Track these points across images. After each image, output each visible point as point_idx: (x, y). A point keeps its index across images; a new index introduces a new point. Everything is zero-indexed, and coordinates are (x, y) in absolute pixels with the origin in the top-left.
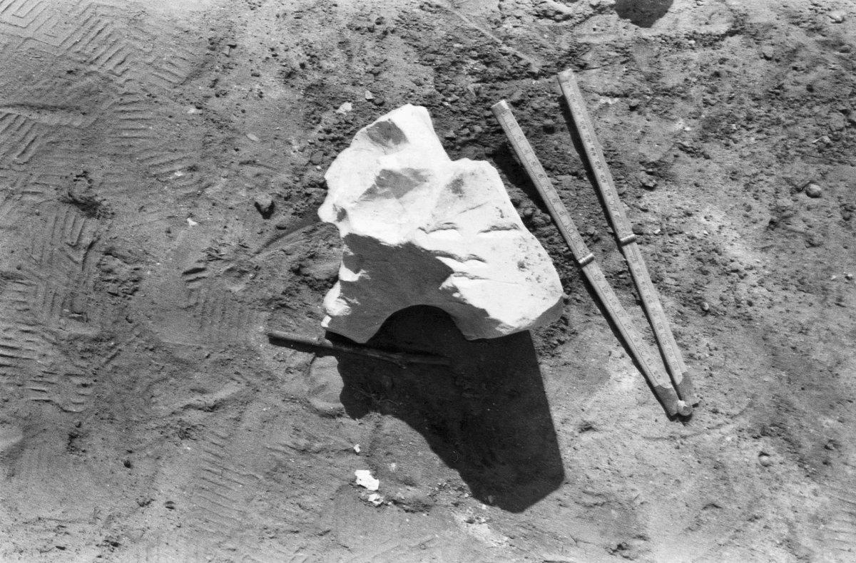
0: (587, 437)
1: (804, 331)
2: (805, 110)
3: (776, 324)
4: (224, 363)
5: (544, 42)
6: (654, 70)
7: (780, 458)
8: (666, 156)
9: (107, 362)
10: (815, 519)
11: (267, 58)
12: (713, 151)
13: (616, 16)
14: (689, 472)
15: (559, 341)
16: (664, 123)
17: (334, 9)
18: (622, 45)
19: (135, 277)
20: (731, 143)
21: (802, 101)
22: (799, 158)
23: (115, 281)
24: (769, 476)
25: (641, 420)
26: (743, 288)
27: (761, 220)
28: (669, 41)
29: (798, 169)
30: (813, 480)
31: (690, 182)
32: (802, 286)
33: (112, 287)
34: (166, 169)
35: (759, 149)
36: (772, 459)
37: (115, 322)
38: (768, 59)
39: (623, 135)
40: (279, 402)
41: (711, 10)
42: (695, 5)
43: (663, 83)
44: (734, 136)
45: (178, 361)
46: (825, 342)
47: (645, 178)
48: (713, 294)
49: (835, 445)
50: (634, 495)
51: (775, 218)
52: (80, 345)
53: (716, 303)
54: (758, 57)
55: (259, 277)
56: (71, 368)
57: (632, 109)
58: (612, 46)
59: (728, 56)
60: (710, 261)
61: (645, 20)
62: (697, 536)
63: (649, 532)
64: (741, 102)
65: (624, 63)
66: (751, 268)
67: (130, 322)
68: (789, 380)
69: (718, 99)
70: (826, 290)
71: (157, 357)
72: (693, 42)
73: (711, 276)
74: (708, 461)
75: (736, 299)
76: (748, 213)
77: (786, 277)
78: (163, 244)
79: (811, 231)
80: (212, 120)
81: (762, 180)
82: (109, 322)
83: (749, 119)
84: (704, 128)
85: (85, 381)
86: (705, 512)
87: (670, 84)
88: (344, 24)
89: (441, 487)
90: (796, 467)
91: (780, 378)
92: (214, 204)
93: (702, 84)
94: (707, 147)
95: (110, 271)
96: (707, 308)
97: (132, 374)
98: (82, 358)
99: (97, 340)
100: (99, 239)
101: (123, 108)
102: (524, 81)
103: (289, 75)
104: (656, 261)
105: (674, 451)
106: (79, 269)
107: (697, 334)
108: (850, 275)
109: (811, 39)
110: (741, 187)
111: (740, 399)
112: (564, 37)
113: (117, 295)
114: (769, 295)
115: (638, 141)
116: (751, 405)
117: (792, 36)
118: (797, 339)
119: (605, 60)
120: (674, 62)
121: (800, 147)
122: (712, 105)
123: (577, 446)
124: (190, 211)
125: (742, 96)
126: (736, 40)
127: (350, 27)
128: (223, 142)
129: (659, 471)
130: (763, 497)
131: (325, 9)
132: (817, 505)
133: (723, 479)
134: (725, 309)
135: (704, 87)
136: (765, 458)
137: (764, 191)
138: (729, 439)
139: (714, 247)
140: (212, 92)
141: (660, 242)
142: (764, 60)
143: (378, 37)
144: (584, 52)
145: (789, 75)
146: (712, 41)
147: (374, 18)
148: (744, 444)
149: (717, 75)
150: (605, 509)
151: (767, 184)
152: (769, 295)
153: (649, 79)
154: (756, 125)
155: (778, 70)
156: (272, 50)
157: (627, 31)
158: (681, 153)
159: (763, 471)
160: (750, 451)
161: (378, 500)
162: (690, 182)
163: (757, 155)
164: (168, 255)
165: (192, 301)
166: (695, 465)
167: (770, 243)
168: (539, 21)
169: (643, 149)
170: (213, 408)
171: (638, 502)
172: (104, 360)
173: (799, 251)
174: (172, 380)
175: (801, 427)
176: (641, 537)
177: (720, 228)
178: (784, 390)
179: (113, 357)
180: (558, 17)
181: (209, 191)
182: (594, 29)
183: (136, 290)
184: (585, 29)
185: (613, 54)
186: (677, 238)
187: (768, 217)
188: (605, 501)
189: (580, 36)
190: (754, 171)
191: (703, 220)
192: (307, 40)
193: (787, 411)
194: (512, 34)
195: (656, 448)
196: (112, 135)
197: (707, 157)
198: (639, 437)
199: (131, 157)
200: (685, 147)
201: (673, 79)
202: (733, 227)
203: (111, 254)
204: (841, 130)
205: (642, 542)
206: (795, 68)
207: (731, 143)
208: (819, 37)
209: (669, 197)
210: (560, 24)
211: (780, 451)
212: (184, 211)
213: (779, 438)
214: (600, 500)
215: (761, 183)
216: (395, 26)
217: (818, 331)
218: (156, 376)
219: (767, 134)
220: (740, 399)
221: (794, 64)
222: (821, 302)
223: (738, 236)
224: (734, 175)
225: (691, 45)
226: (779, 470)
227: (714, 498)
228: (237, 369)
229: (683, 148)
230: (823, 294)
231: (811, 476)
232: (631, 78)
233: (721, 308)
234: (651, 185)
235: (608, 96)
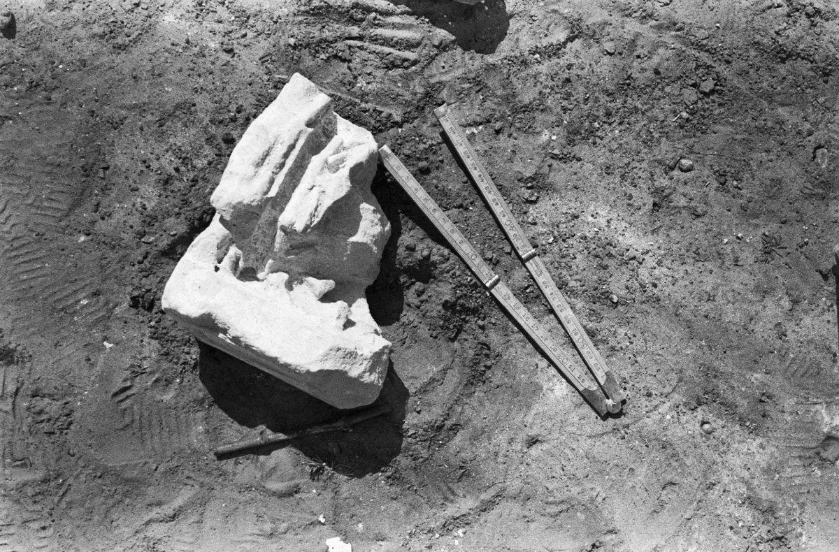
0: (535, 451)
1: (711, 298)
2: (657, 93)
3: (684, 298)
4: (173, 471)
5: (400, 91)
6: (509, 91)
7: (721, 423)
8: (540, 168)
9: (59, 501)
10: (767, 471)
11: (142, 171)
12: (584, 152)
13: (459, 50)
14: (640, 458)
15: (485, 366)
16: (531, 139)
17: (193, 109)
18: (473, 75)
19: (66, 411)
20: (598, 141)
21: (652, 85)
22: (664, 139)
23: (49, 420)
24: (715, 442)
25: (582, 421)
26: (643, 273)
27: (645, 205)
28: (515, 60)
29: (664, 149)
30: (757, 435)
31: (569, 187)
32: (699, 257)
33: (46, 427)
34: (71, 301)
35: (625, 139)
36: (714, 425)
37: (58, 460)
38: (611, 54)
39: (497, 159)
40: (235, 495)
41: (546, 22)
42: (531, 22)
43: (520, 101)
45: (128, 481)
46: (733, 304)
47: (527, 194)
48: (617, 286)
49: (768, 397)
50: (595, 494)
51: (657, 199)
52: (30, 491)
53: (623, 293)
54: (601, 54)
55: (186, 380)
56: (26, 516)
57: (498, 132)
58: (463, 78)
59: (573, 60)
60: (607, 255)
61: (488, 47)
62: (664, 515)
63: (618, 525)
64: (597, 100)
65: (477, 92)
66: (647, 252)
67: (73, 456)
68: (710, 347)
69: (575, 103)
70: (722, 254)
71: (108, 482)
72: (537, 56)
73: (612, 269)
74: (654, 443)
75: (640, 284)
76: (631, 202)
77: (683, 251)
78: (85, 373)
79: (693, 204)
80: (104, 242)
81: (636, 168)
82: (52, 461)
83: (608, 114)
84: (569, 132)
85: (43, 524)
86: (665, 492)
87: (527, 101)
88: (207, 120)
89: (411, 535)
90: (737, 427)
91: (701, 347)
92: (126, 322)
93: (557, 93)
94: (576, 150)
95: (40, 412)
96: (615, 299)
97: (87, 505)
98: (35, 502)
99: (45, 481)
100: (23, 384)
101: (14, 254)
102: (391, 131)
103: (166, 182)
104: (557, 268)
105: (620, 441)
106: (10, 418)
107: (613, 326)
108: (740, 235)
109: (646, 26)
110: (618, 179)
111: (669, 377)
112: (417, 81)
113: (53, 433)
114: (669, 273)
115: (511, 160)
116: (680, 380)
117: (628, 27)
118: (705, 307)
119: (461, 93)
120: (525, 79)
121: (662, 128)
123: (529, 460)
124: (105, 334)
125: (597, 94)
126: (577, 44)
127: (212, 122)
128: (120, 261)
129: (611, 465)
130: (714, 463)
131: (185, 111)
132: (767, 458)
133: (673, 456)
134: (633, 296)
135: (559, 95)
136: (706, 427)
137: (640, 177)
138: (668, 417)
139: (607, 241)
140: (97, 216)
141: (556, 249)
142: (608, 56)
143: (242, 124)
144: (439, 91)
145: (635, 64)
146: (555, 51)
147: (233, 107)
148: (684, 419)
149: (568, 80)
150: (570, 513)
151: (641, 170)
152: (669, 273)
153: (507, 99)
154: (616, 118)
155: (623, 61)
156: (145, 162)
157: (474, 62)
158: (555, 163)
159: (708, 439)
160: (691, 424)
162: (569, 187)
163: (626, 146)
164: (94, 382)
165: (127, 420)
166: (644, 450)
167: (658, 224)
168: (390, 72)
169: (517, 167)
170: (173, 518)
171: (600, 499)
172: (56, 499)
173: (686, 225)
174: (127, 501)
175: (733, 388)
176: (610, 532)
177: (608, 222)
178: (709, 358)
179: (66, 492)
180: (406, 64)
181: (117, 310)
182: (443, 67)
183: (71, 423)
184: (434, 69)
185: (466, 86)
186: (570, 241)
187: (650, 201)
188: (569, 506)
189: (431, 76)
190: (626, 161)
191: (590, 219)
192: (175, 144)
193: (715, 376)
194: (367, 90)
195: (604, 443)
196: (12, 281)
197: (579, 160)
198: (584, 437)
199: (34, 297)
200: (555, 155)
201: (528, 96)
202: (621, 218)
203: (38, 396)
204: (696, 103)
205: (614, 536)
206: (638, 57)
207: (598, 141)
208: (653, 23)
209: (553, 205)
210: (409, 71)
211: (719, 416)
212: (98, 336)
213: (714, 404)
214: (564, 507)
216: (255, 111)
217: (724, 294)
218: (111, 502)
219: (629, 124)
220: (669, 377)
221: (635, 54)
222: (720, 267)
223: (628, 226)
224: (608, 170)
225: (536, 59)
226: (721, 434)
227: (669, 477)
228: (186, 472)
229: (554, 157)
230: (720, 258)
231: (755, 431)
232: (488, 104)
233: (629, 296)
234: (534, 198)
235: (472, 126)
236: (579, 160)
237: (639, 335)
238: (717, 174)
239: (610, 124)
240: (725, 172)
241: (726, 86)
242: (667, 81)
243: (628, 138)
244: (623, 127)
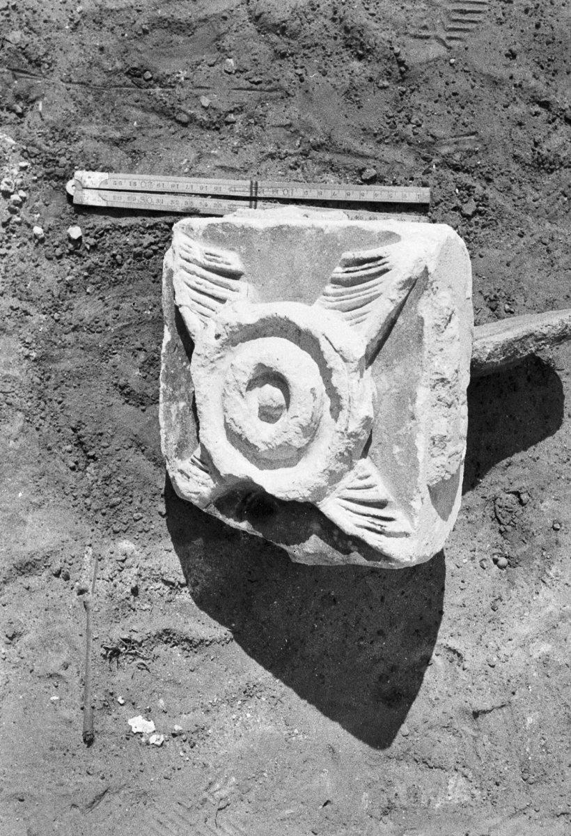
238: (488, 300)
240: (495, 296)
241: (488, 206)
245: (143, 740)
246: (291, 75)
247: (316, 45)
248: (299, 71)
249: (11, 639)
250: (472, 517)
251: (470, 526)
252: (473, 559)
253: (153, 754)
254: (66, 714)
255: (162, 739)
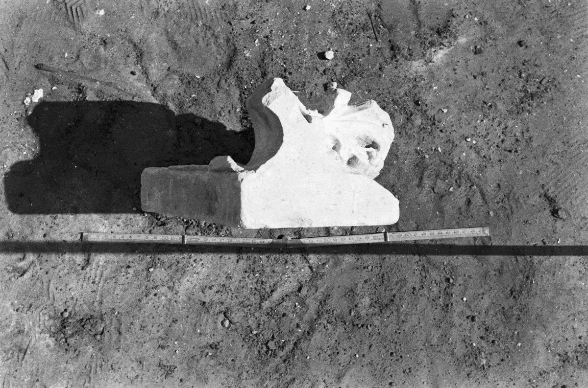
1: (142, 328)
20: (247, 275)
26: (164, 289)
44: (252, 275)
49: (77, 355)
64: (272, 277)
73: (169, 271)
76: (207, 288)
81: (228, 294)
96: (150, 270)
108: (177, 352)
122: (268, 261)
126: (307, 269)
161: (27, 102)
187: (207, 300)
197: (238, 261)
207: (247, 275)
215: (226, 294)
219: (255, 294)
236: (238, 261)
237: (127, 281)
238: (217, 344)
239: (256, 283)
240: (218, 349)
241: (270, 357)
242: (278, 321)
243: (246, 292)
244: (254, 289)
245: (29, 94)
246: (369, 263)
247: (383, 282)
248: (370, 267)
249: (104, 41)
250: (96, 304)
251: (92, 301)
252: (72, 298)
253: (21, 98)
254: (56, 59)
255: (27, 104)
